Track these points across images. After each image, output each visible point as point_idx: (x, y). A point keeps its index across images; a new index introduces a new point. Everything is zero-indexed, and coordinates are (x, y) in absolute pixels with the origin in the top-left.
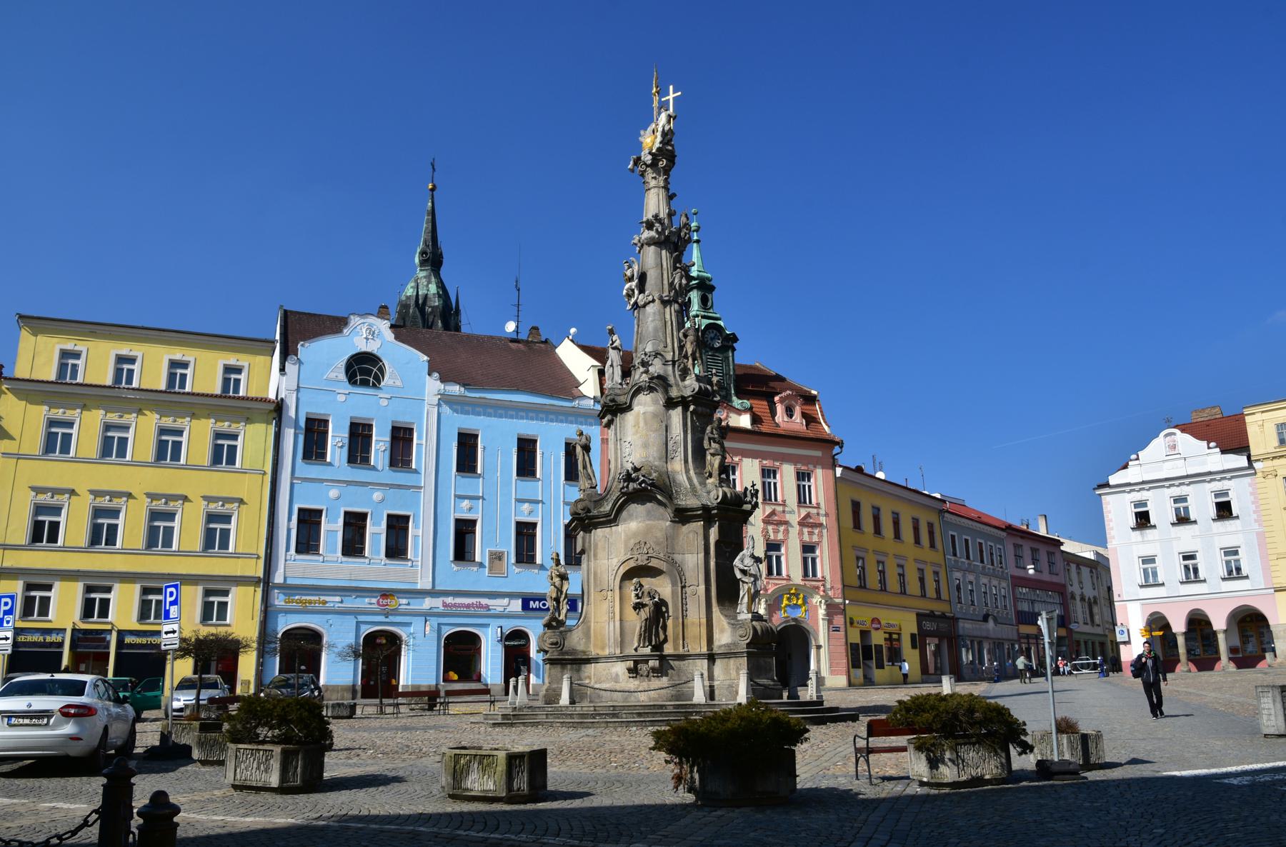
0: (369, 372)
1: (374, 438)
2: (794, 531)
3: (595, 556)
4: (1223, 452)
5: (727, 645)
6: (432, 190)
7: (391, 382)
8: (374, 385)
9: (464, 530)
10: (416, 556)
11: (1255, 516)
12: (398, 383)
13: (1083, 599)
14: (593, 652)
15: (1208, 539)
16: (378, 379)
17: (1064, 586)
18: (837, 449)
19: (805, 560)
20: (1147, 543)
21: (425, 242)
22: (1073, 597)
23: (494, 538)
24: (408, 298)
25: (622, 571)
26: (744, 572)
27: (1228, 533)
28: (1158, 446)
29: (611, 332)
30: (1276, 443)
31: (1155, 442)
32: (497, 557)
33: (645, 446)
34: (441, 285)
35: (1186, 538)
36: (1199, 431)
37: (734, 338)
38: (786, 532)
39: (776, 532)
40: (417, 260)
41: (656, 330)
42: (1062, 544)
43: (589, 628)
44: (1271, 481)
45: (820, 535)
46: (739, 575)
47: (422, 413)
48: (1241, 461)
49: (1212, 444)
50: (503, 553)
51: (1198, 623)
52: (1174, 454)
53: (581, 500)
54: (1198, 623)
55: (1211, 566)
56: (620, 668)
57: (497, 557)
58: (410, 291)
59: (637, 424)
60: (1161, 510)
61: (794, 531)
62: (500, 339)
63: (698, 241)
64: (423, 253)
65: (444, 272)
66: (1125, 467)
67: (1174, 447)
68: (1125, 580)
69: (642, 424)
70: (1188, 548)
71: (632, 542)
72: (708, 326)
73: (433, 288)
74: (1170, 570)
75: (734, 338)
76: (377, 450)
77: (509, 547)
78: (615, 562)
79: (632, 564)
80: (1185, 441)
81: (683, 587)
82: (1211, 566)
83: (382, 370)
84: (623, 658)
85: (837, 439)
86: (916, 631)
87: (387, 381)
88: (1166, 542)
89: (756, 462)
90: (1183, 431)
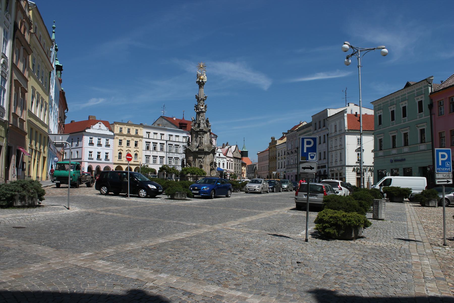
15: (103, 150)
20: (91, 148)
31: (97, 124)
35: (99, 149)
36: (107, 124)
44: (117, 139)
48: (112, 134)
51: (98, 168)
54: (98, 168)
55: (103, 156)
60: (95, 140)
63: (54, 32)
66: (89, 128)
67: (100, 126)
74: (95, 156)
80: (103, 126)
82: (103, 156)
88: (95, 149)
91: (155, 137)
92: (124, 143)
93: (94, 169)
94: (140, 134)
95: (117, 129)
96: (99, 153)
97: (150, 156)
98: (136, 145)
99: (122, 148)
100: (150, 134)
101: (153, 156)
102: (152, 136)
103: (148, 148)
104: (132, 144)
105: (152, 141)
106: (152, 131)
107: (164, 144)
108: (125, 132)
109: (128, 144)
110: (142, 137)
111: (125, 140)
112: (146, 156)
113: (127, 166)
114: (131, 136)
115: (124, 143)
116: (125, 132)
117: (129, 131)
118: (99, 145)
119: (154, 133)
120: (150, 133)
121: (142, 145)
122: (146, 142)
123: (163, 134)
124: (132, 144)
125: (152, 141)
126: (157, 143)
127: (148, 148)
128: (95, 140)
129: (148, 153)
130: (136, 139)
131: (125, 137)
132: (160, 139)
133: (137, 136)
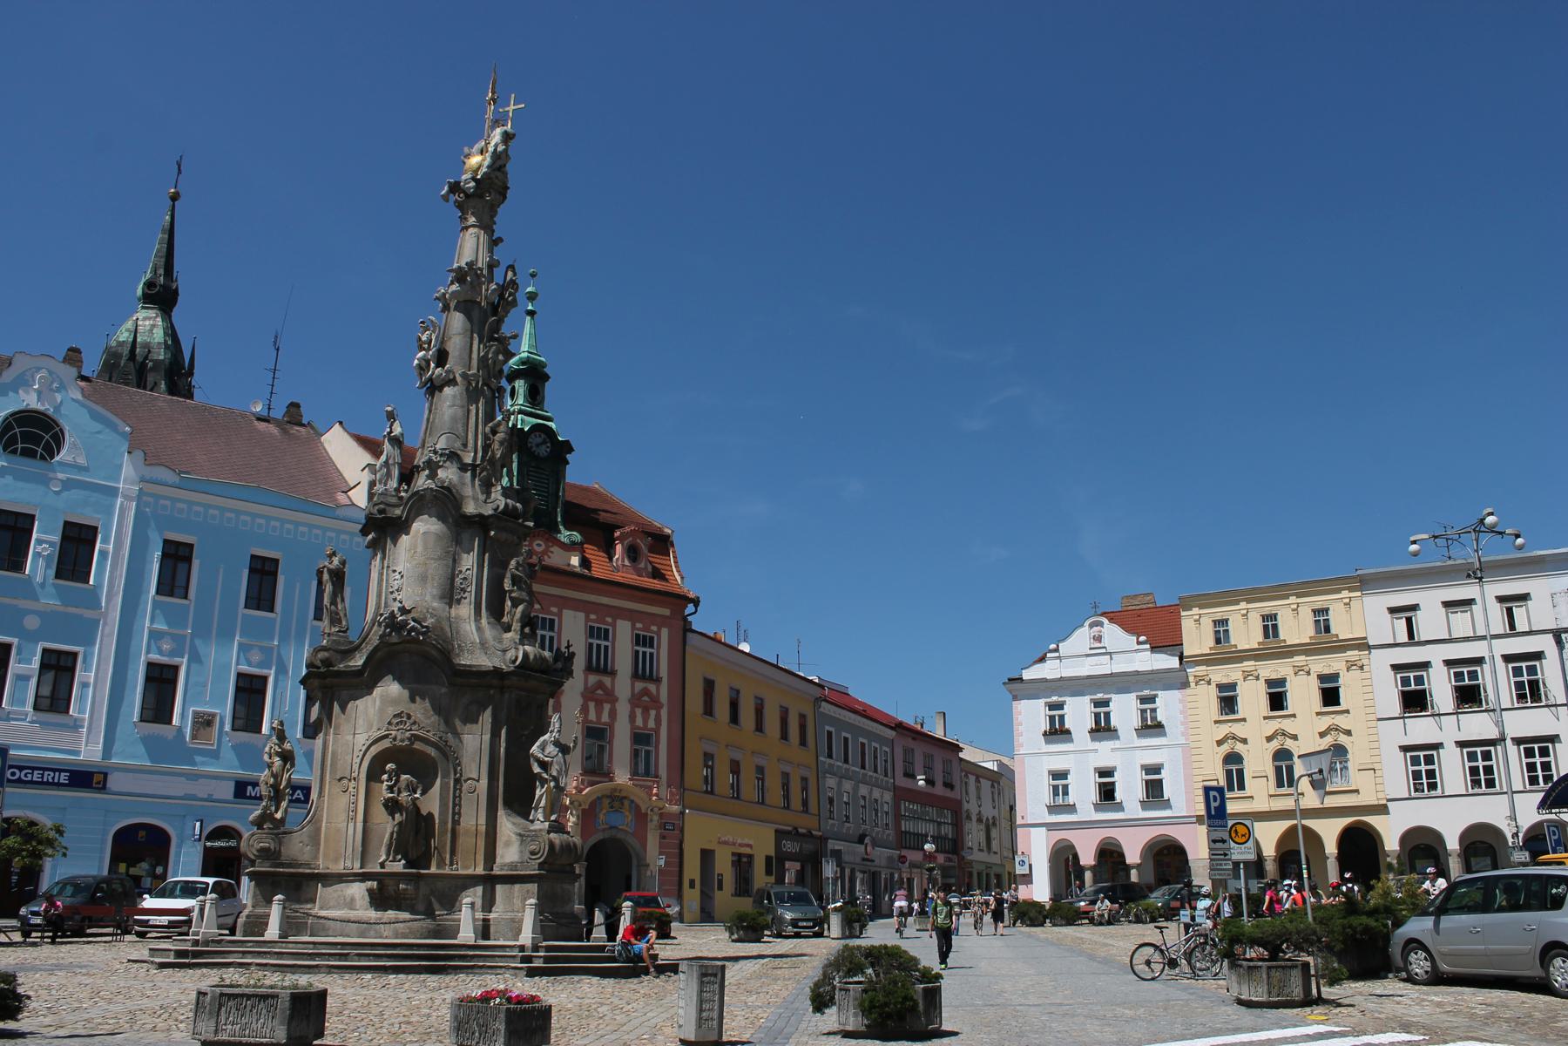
0: (36, 440)
1: (34, 536)
2: (623, 708)
3: (337, 727)
4: (1154, 649)
5: (513, 866)
6: (175, 198)
7: (69, 459)
8: (43, 458)
9: (161, 680)
10: (82, 711)
11: (1182, 728)
12: (81, 461)
13: (980, 820)
14: (323, 865)
16: (51, 450)
17: (959, 803)
18: (690, 608)
19: (636, 754)
21: (155, 270)
22: (969, 818)
23: (205, 693)
24: (121, 344)
25: (374, 750)
26: (544, 765)
27: (1153, 751)
28: (1080, 639)
29: (391, 416)
30: (1212, 643)
32: (204, 722)
33: (423, 579)
34: (171, 332)
35: (1105, 753)
36: (1129, 620)
37: (567, 447)
38: (613, 714)
39: (599, 712)
40: (139, 292)
41: (454, 419)
42: (961, 750)
43: (318, 830)
44: (1203, 687)
45: (658, 720)
46: (536, 769)
47: (112, 506)
49: (1142, 638)
50: (214, 715)
51: (1110, 855)
52: (1098, 649)
53: (324, 649)
54: (1110, 855)
55: (1130, 789)
56: (358, 890)
57: (204, 722)
58: (124, 335)
59: (414, 546)
60: (1079, 713)
61: (623, 708)
62: (243, 416)
63: (531, 313)
64: (150, 285)
65: (176, 313)
66: (1042, 659)
67: (1098, 639)
68: (1032, 800)
69: (420, 549)
70: (1105, 763)
71: (391, 711)
72: (535, 428)
73: (159, 335)
74: (1083, 791)
75: (567, 447)
76: (37, 555)
77: (225, 709)
78: (362, 740)
79: (386, 744)
80: (1113, 635)
81: (457, 781)
82: (1130, 789)
83: (58, 439)
84: (364, 877)
85: (691, 595)
86: (772, 853)
87: (63, 455)
89: (581, 615)
90: (1111, 620)
91: (1461, 623)
92: (1253, 698)
93: (1087, 858)
94: (1342, 627)
95: (1196, 634)
96: (1105, 773)
97: (1437, 746)
98: (1330, 696)
99: (1238, 729)
100: (1420, 618)
101: (1462, 744)
102: (1431, 621)
103: (1415, 701)
104: (1303, 694)
105: (1436, 655)
106: (1429, 600)
107: (1538, 656)
108: (1245, 633)
109: (1277, 701)
110: (1363, 645)
111: (1251, 683)
112: (1405, 749)
113: (1284, 825)
114: (1289, 652)
115: (1253, 698)
116: (1245, 633)
117: (1270, 627)
118: (1103, 729)
119: (1447, 604)
120: (1414, 608)
121: (1372, 689)
122: (1396, 668)
123: (1524, 597)
124: (1303, 694)
125: (1436, 655)
126: (1425, 665)
127: (1415, 701)
128: (1079, 713)
129: (1421, 729)
130: (1270, 669)
131: (1249, 665)
132: (1499, 625)
133: (1325, 640)
